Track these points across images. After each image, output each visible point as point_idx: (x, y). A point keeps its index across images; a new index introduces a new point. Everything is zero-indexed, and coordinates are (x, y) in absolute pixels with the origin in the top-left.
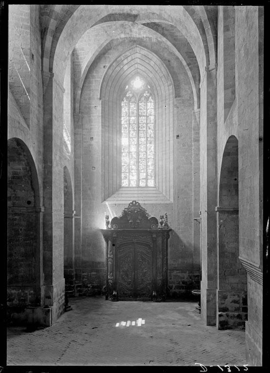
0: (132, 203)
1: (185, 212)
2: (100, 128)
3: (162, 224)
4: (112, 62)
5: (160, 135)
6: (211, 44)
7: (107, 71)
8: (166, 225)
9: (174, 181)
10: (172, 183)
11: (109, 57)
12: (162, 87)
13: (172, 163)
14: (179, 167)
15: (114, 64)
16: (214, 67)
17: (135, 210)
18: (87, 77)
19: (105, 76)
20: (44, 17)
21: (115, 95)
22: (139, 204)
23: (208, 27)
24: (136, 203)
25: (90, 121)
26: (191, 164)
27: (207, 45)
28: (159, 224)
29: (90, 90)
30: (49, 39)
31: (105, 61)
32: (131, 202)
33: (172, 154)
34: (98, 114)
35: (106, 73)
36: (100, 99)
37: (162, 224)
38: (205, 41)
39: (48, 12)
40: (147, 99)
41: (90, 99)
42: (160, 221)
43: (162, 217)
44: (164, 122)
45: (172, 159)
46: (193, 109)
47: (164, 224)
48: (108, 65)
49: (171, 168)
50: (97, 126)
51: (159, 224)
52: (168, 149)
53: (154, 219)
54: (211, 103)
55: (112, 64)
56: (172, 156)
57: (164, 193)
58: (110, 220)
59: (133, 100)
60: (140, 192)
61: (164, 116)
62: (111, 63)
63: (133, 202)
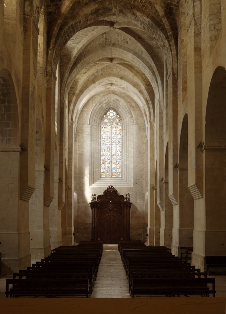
0: (109, 187)
1: (140, 193)
2: (89, 142)
3: (126, 199)
4: (97, 103)
5: (125, 146)
6: (152, 110)
7: (94, 107)
8: (129, 200)
9: (134, 174)
10: (132, 175)
11: (95, 100)
12: (127, 118)
13: (132, 163)
14: (136, 166)
15: (98, 104)
16: (153, 121)
17: (111, 191)
18: (82, 111)
19: (92, 111)
20: (70, 95)
21: (98, 121)
22: (113, 187)
23: (150, 103)
24: (112, 187)
25: (83, 137)
26: (144, 164)
27: (150, 110)
28: (125, 199)
29: (83, 119)
30: (72, 105)
31: (93, 102)
32: (109, 186)
33: (132, 158)
34: (87, 133)
35: (93, 109)
36: (89, 124)
37: (126, 199)
38: (149, 108)
39: (73, 93)
40: (117, 124)
41: (83, 124)
42: (125, 197)
43: (126, 195)
44: (128, 139)
45: (132, 161)
46: (145, 132)
47: (127, 199)
48: (94, 105)
49: (132, 166)
50: (87, 141)
51: (125, 199)
52: (130, 154)
53: (122, 196)
54: (152, 138)
55: (97, 104)
56: (133, 159)
57: (128, 182)
58: (96, 197)
59: (109, 124)
60: (116, 182)
61: (128, 135)
62: (96, 103)
63: (110, 186)
